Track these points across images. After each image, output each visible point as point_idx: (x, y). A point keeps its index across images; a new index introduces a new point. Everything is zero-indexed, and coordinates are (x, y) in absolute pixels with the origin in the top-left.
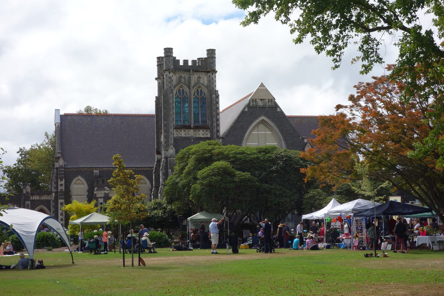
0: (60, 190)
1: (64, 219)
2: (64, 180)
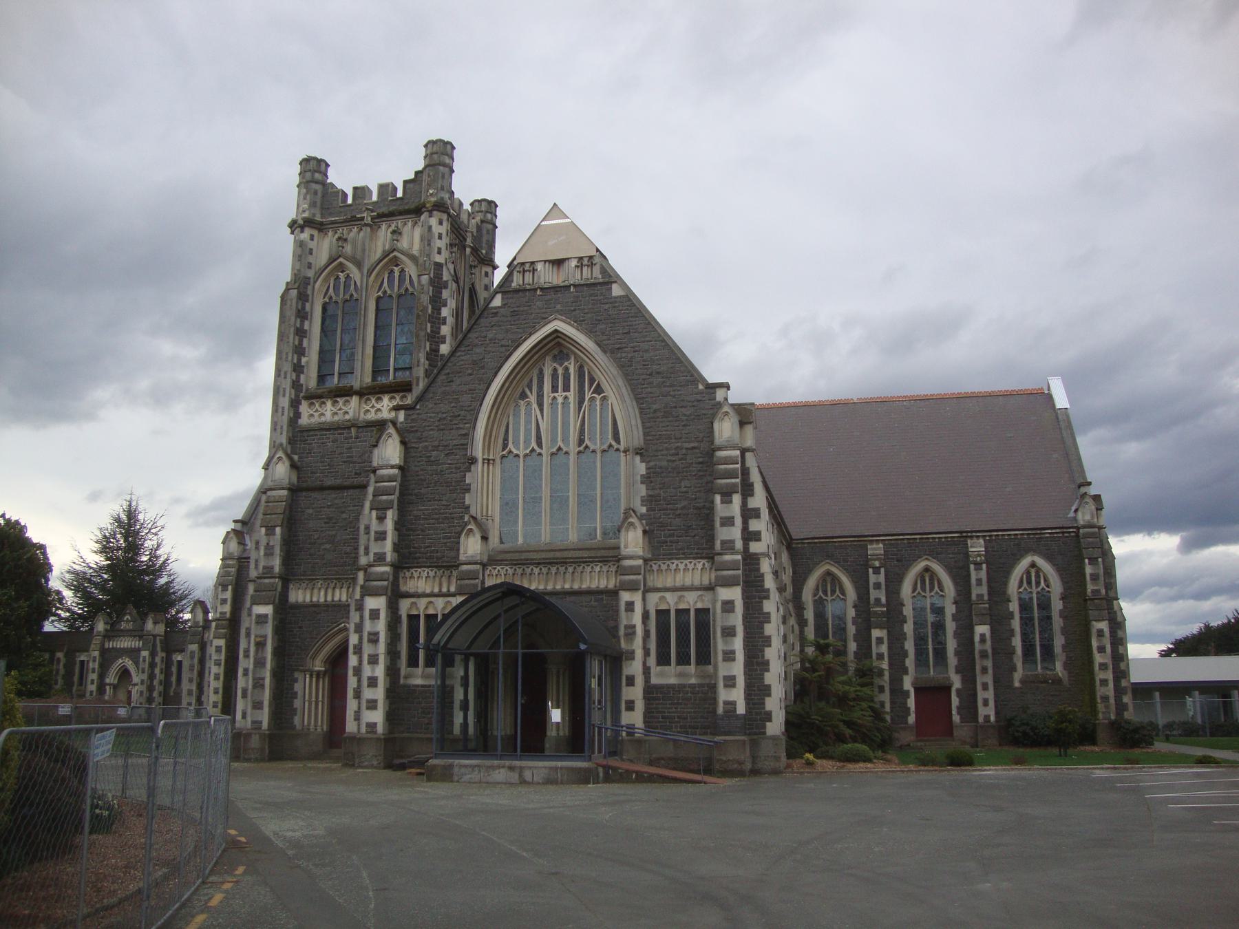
1: (221, 691)
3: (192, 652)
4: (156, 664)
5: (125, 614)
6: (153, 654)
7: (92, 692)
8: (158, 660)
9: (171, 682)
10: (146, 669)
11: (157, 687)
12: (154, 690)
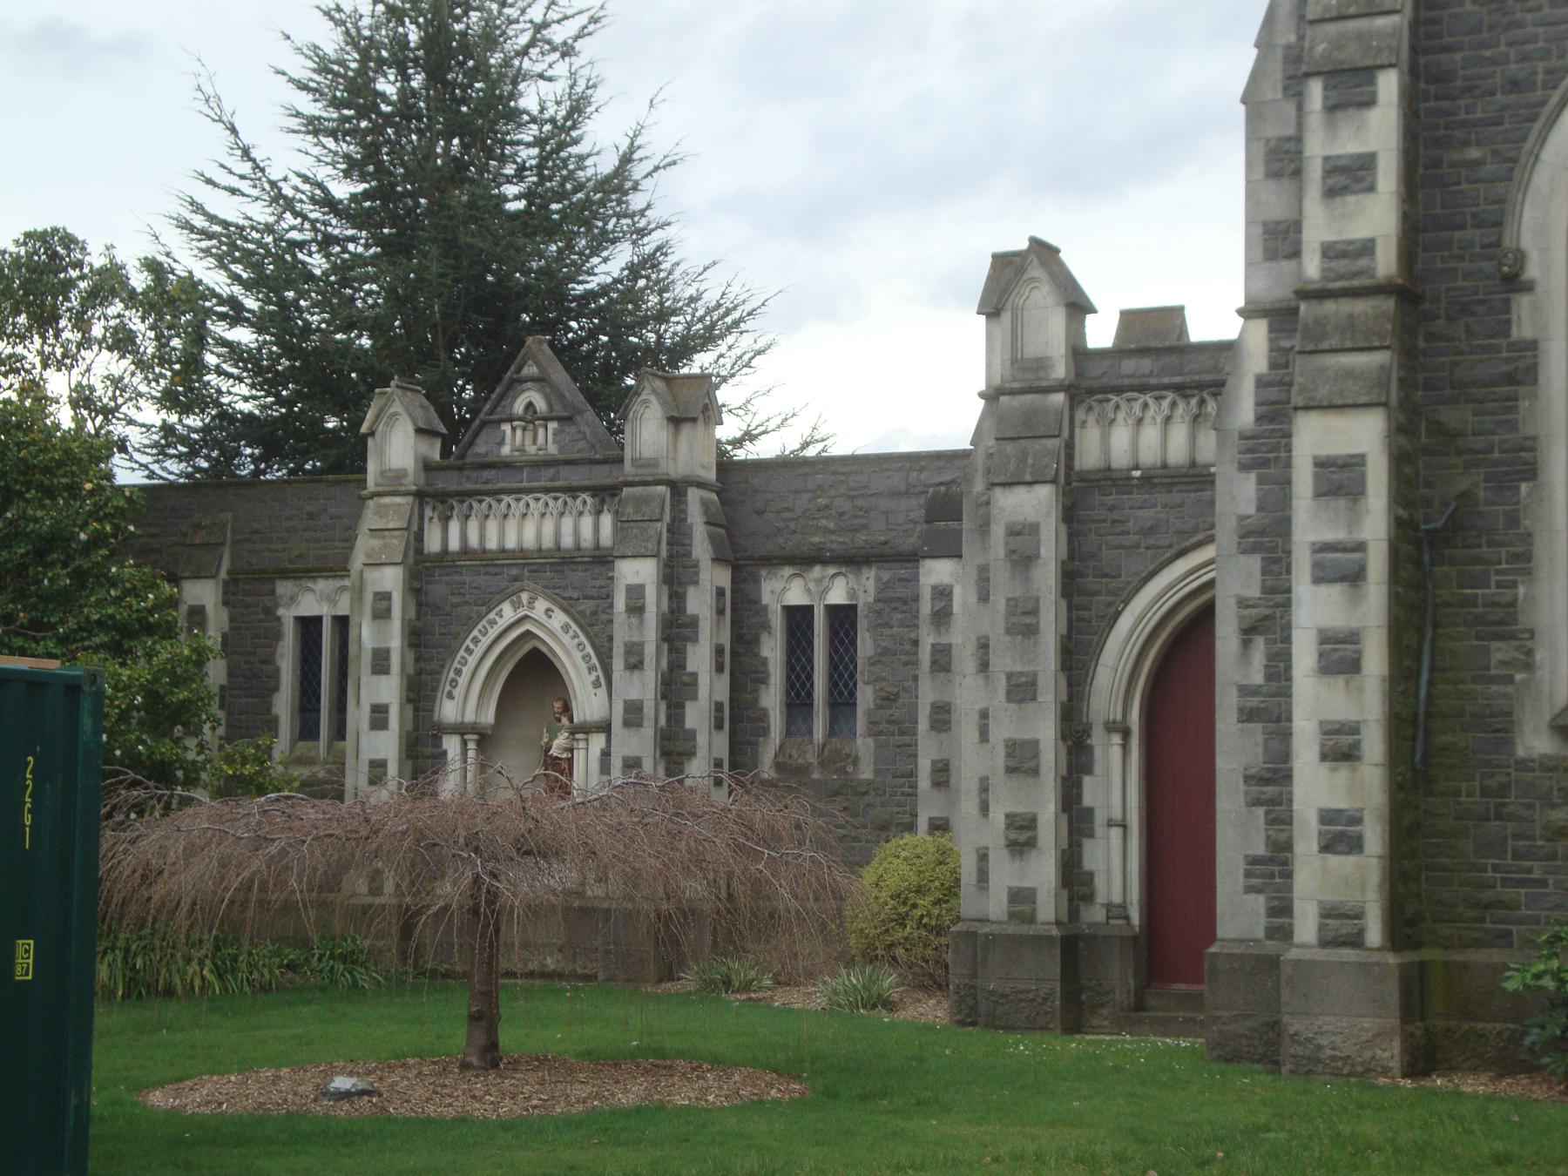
0: (1330, 252)
1: (1374, 745)
2: (1389, 85)
3: (1022, 532)
4: (694, 623)
5: (518, 383)
6: (676, 576)
7: (378, 766)
8: (699, 603)
9: (763, 716)
10: (650, 650)
11: (702, 740)
12: (691, 754)
